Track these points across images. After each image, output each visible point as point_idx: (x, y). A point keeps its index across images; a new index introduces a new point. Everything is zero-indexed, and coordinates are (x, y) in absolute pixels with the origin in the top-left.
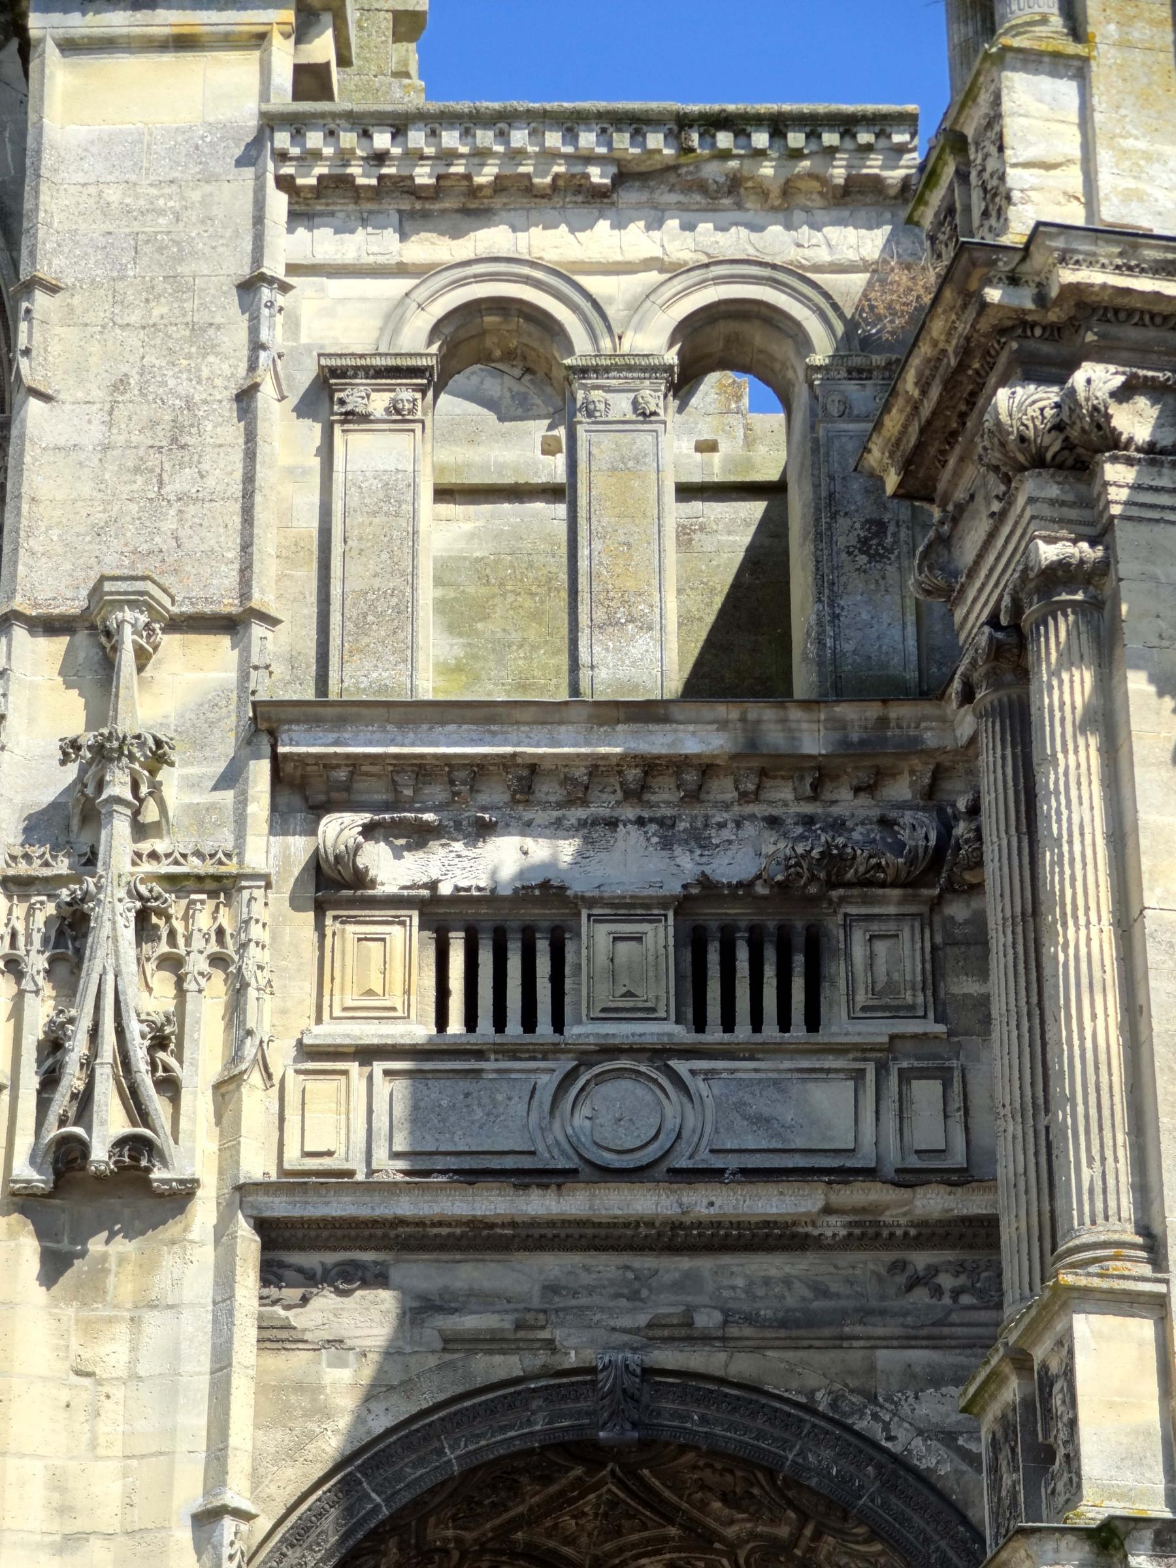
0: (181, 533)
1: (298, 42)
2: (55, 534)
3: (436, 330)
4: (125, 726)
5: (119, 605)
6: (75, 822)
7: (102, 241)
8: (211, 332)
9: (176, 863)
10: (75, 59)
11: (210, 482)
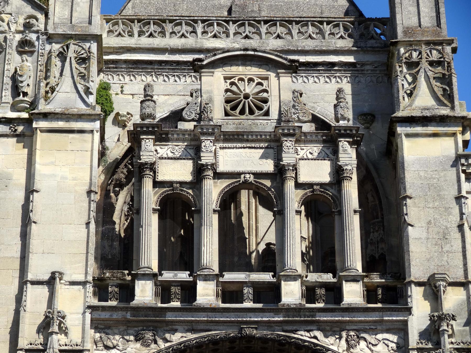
0: (448, 261)
1: (463, 135)
2: (418, 260)
4: (445, 312)
5: (439, 280)
6: (432, 334)
7: (420, 186)
8: (450, 209)
9: (457, 345)
10: (409, 139)
11: (454, 248)
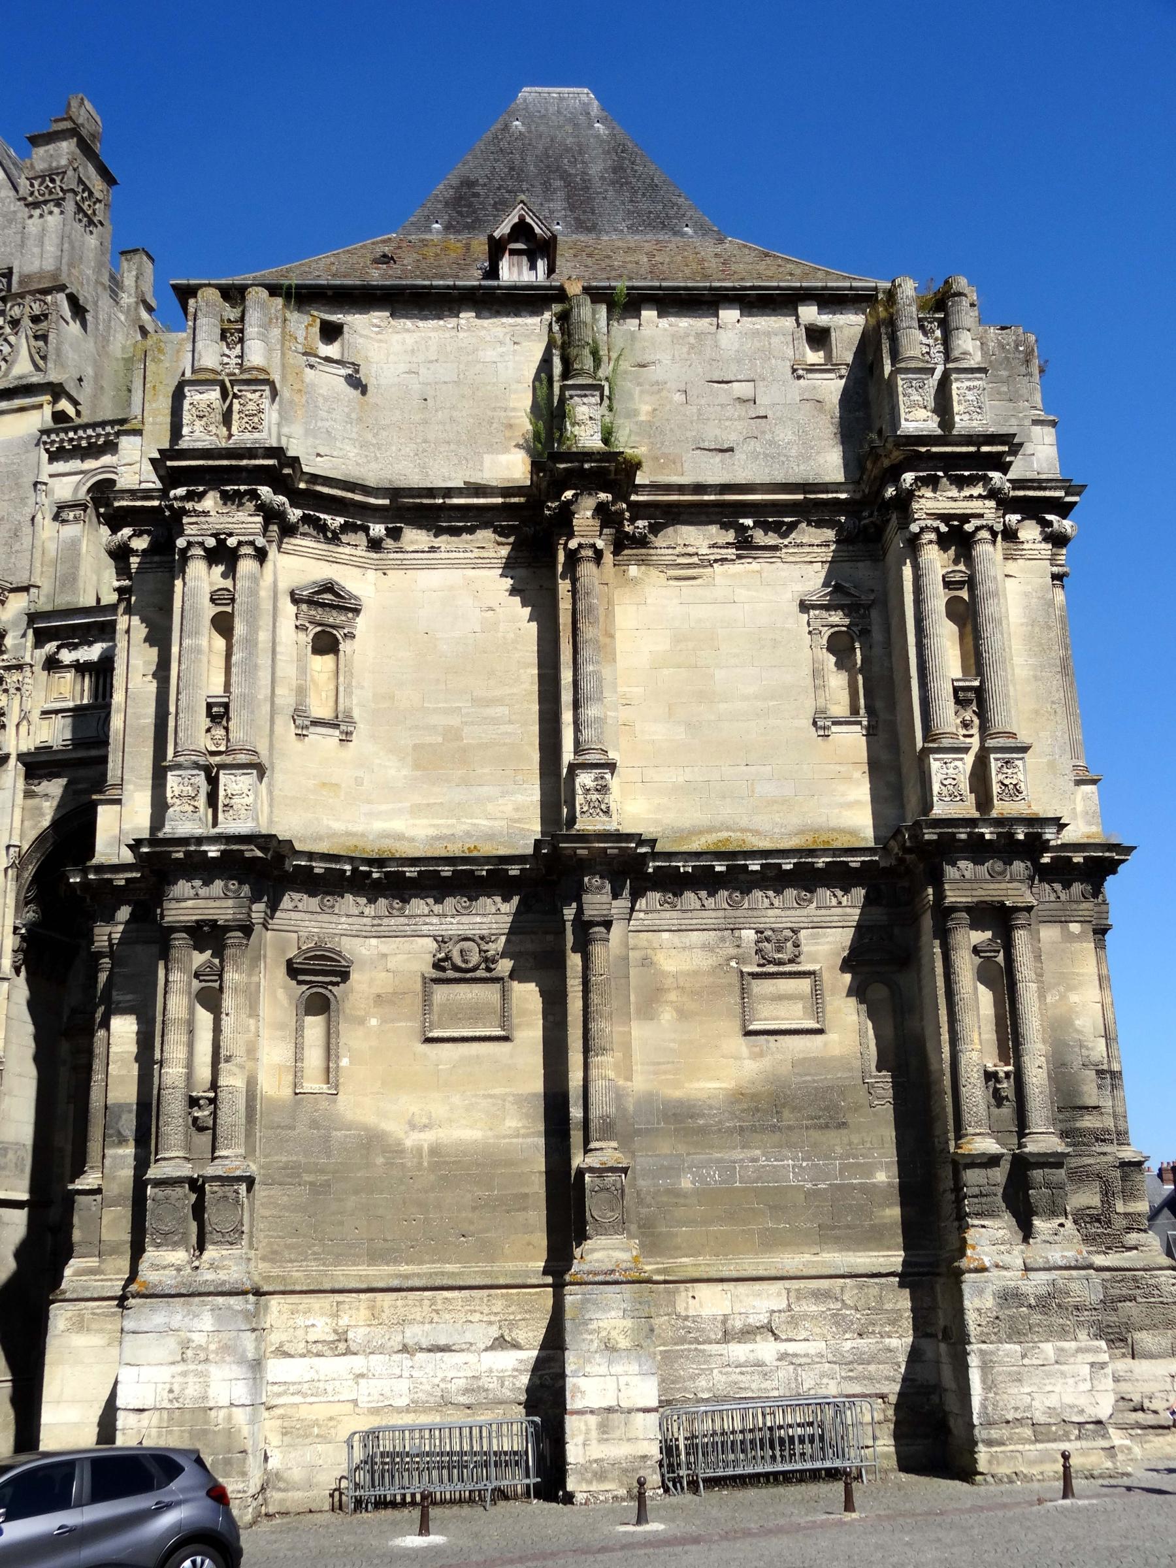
3: (89, 491)
